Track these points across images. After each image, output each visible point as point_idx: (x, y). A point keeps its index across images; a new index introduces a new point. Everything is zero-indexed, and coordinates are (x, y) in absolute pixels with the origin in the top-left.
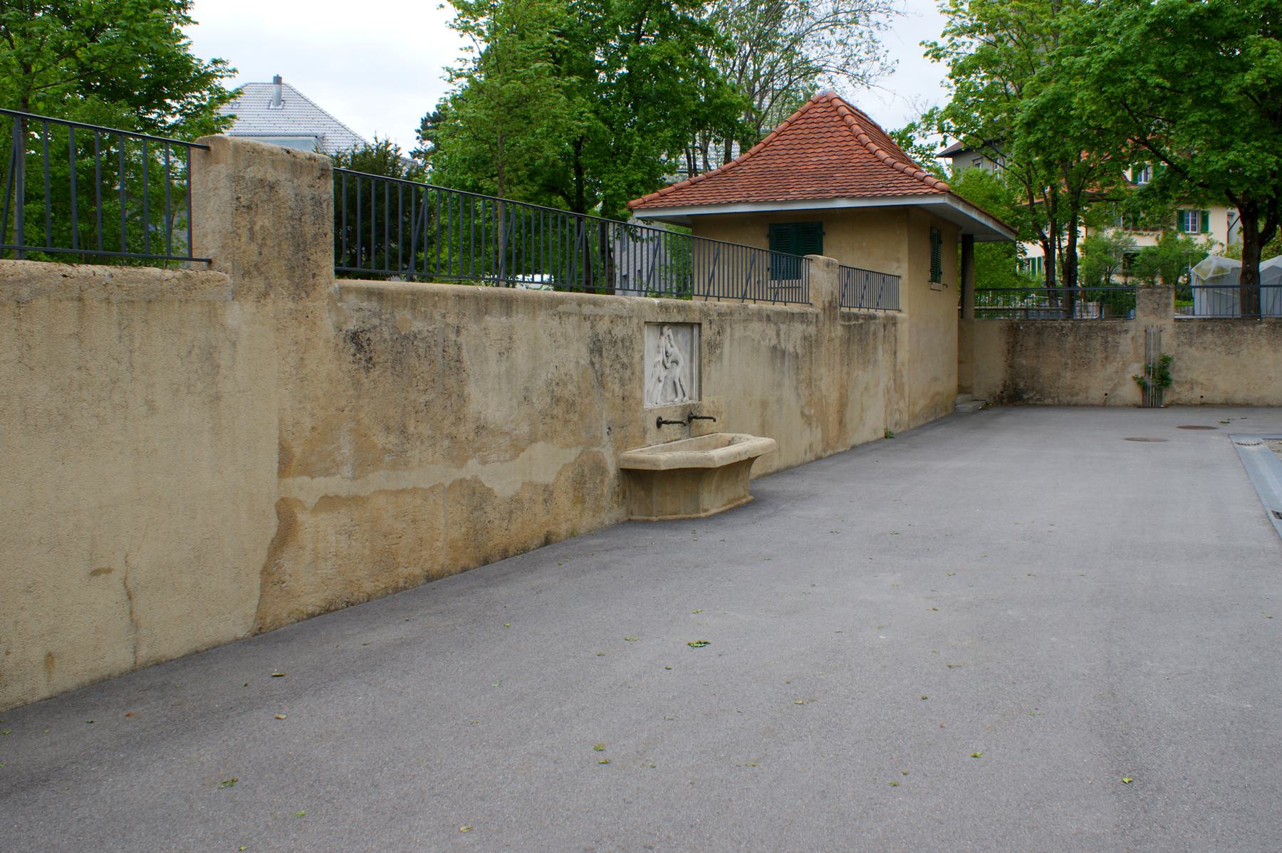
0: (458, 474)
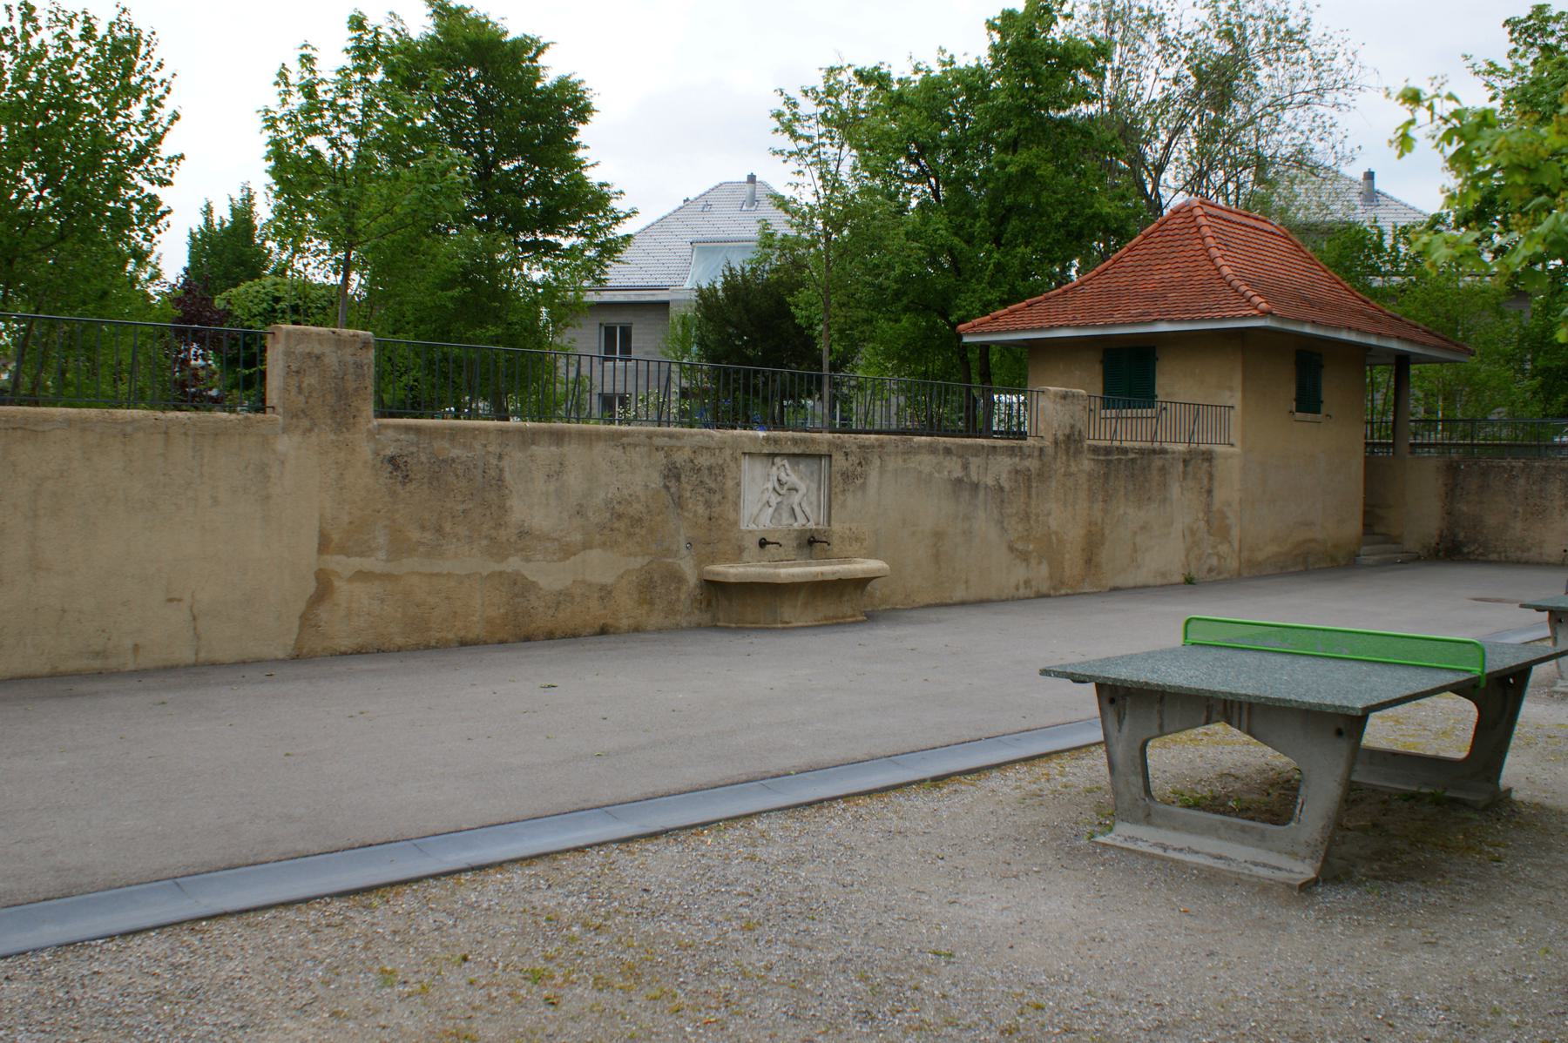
0: (497, 567)
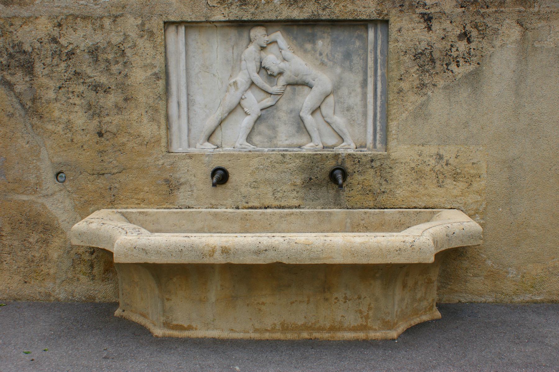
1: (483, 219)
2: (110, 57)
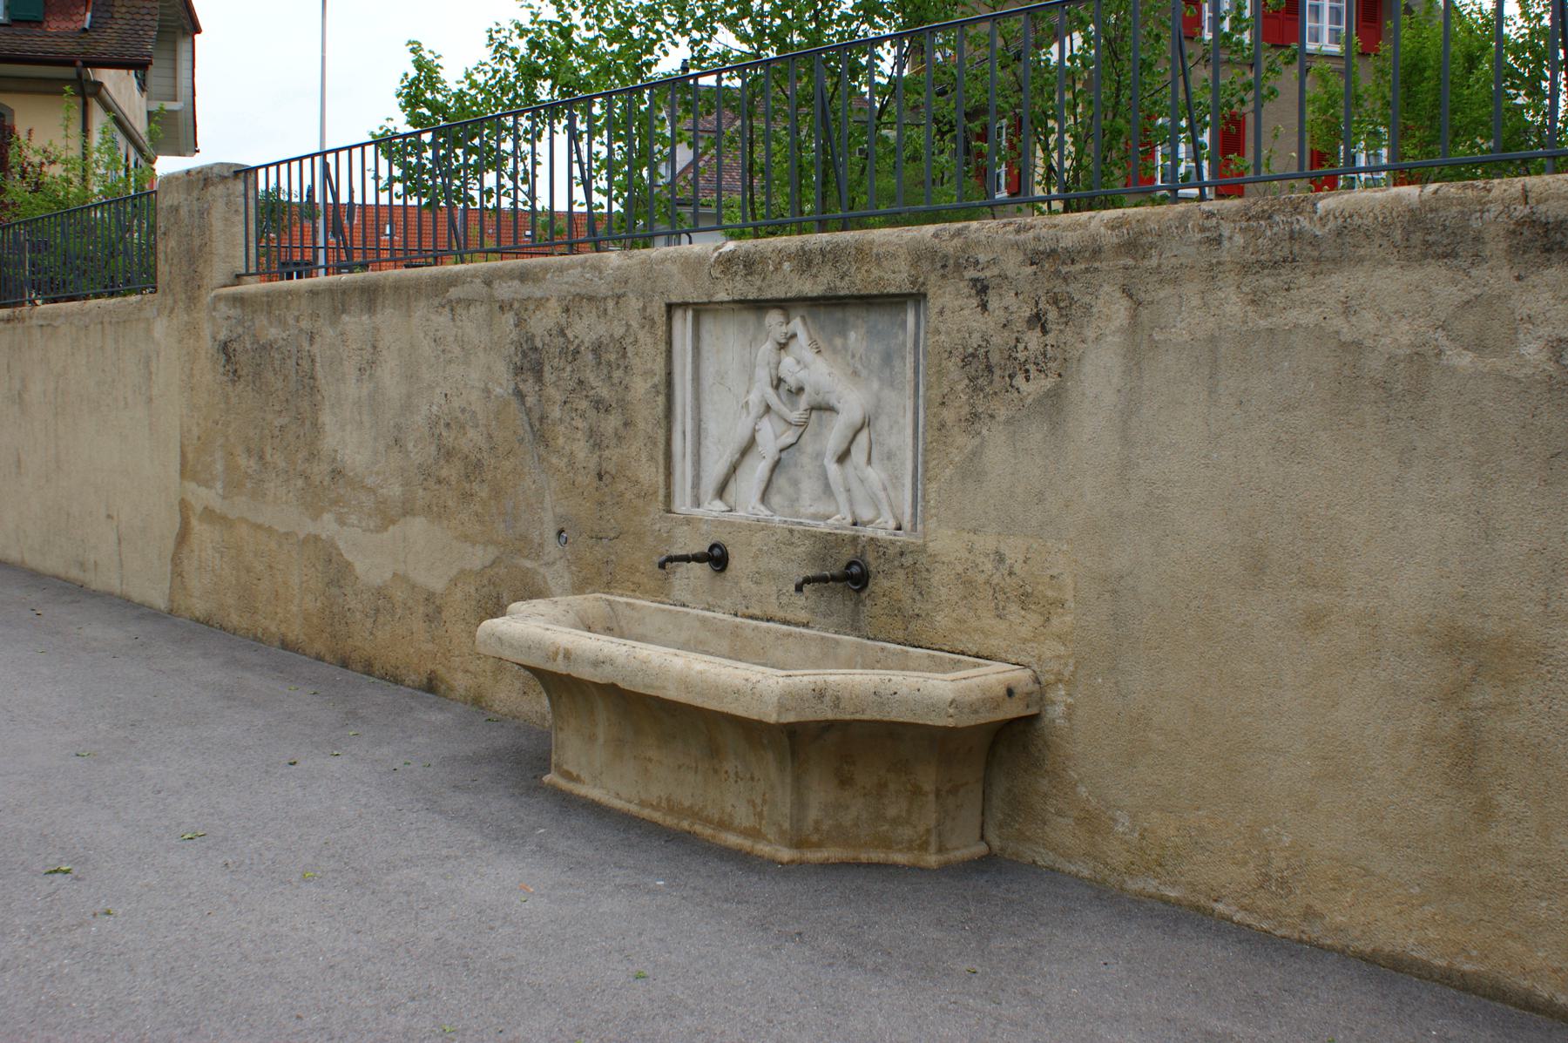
0: (310, 528)
1: (1070, 695)
2: (613, 357)
